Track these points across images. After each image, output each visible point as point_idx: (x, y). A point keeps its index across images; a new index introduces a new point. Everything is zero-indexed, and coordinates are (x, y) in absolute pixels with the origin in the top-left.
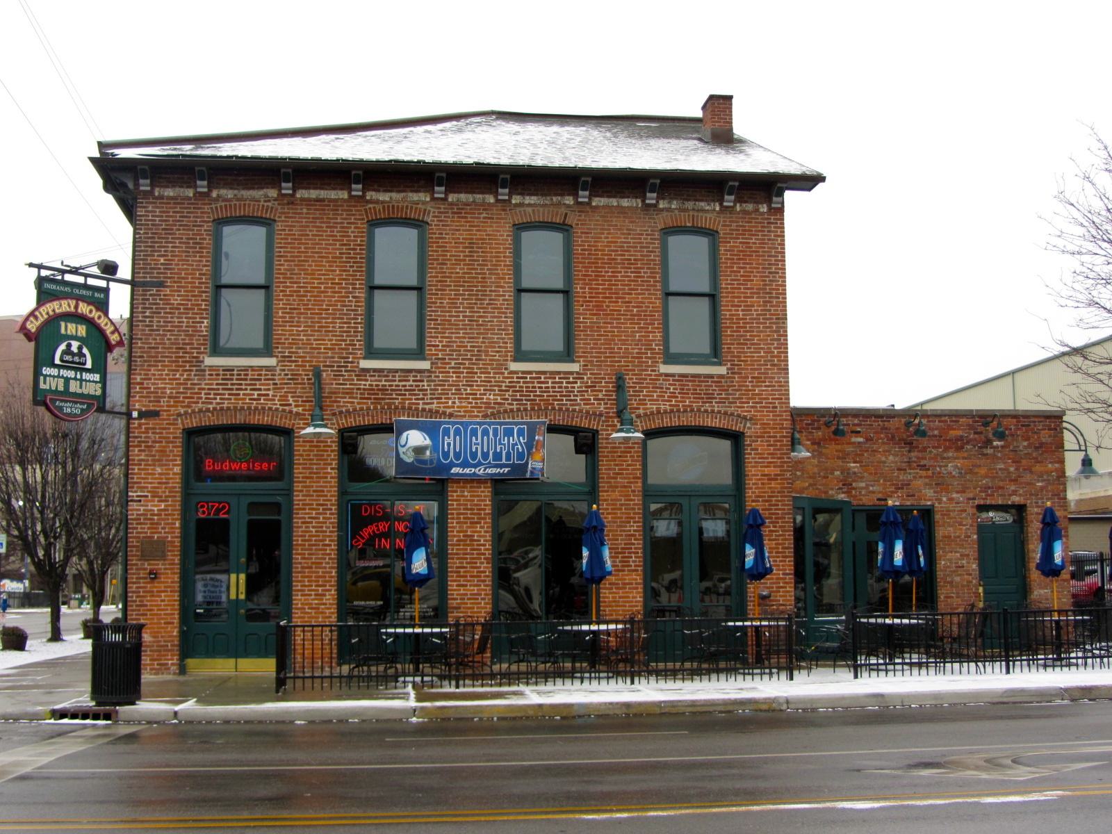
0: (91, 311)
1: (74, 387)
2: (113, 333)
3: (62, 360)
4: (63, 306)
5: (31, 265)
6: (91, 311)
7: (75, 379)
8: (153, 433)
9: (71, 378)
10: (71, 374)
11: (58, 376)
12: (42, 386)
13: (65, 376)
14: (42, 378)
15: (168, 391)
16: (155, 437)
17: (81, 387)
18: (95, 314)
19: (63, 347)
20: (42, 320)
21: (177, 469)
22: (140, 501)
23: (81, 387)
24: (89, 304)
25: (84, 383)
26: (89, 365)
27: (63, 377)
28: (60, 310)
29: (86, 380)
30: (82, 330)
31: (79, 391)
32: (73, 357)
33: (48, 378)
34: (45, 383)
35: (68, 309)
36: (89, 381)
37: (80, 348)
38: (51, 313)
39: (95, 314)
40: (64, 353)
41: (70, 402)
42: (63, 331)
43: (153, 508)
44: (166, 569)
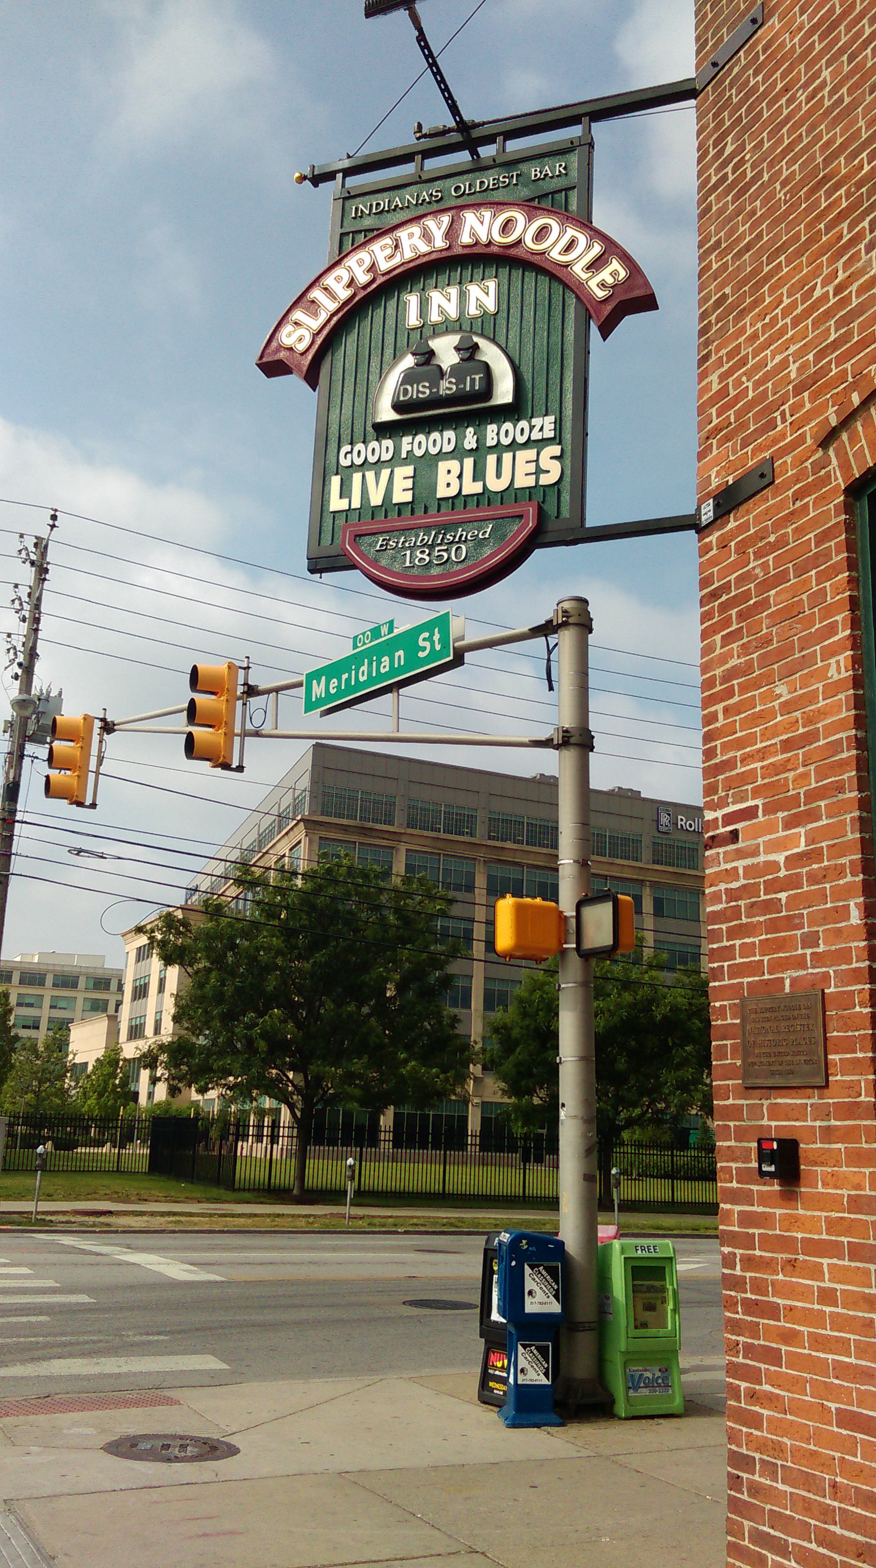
0: (506, 227)
1: (449, 480)
2: (596, 265)
3: (397, 407)
4: (406, 243)
5: (318, 179)
6: (506, 227)
7: (458, 453)
8: (758, 555)
9: (441, 455)
10: (446, 439)
11: (395, 461)
12: (336, 503)
13: (419, 453)
14: (335, 481)
15: (793, 368)
16: (765, 566)
17: (479, 474)
18: (524, 229)
19: (409, 361)
20: (332, 306)
21: (839, 668)
22: (734, 836)
23: (479, 474)
24: (498, 205)
25: (491, 459)
26: (504, 393)
27: (410, 458)
28: (397, 260)
29: (498, 448)
30: (483, 295)
31: (472, 488)
32: (434, 384)
33: (357, 477)
34: (345, 491)
35: (424, 248)
36: (514, 446)
37: (469, 351)
38: (363, 278)
39: (524, 229)
40: (409, 378)
41: (427, 528)
42: (413, 319)
43: (772, 857)
44: (828, 1134)
